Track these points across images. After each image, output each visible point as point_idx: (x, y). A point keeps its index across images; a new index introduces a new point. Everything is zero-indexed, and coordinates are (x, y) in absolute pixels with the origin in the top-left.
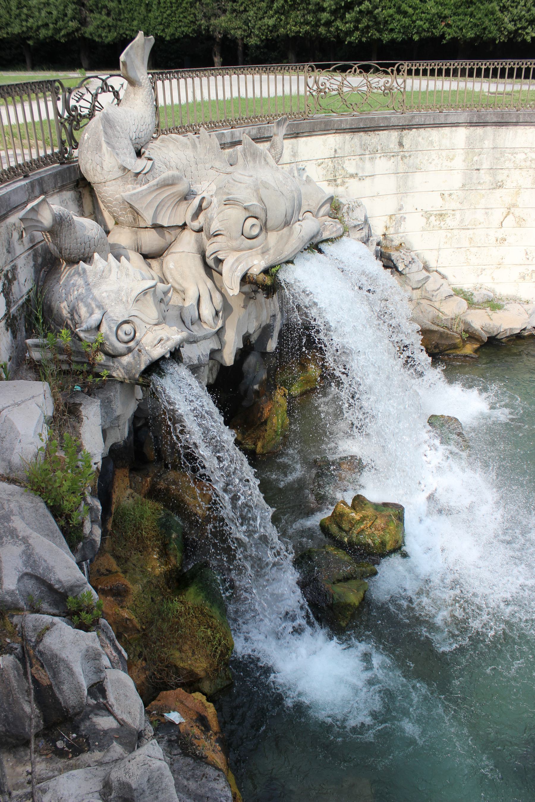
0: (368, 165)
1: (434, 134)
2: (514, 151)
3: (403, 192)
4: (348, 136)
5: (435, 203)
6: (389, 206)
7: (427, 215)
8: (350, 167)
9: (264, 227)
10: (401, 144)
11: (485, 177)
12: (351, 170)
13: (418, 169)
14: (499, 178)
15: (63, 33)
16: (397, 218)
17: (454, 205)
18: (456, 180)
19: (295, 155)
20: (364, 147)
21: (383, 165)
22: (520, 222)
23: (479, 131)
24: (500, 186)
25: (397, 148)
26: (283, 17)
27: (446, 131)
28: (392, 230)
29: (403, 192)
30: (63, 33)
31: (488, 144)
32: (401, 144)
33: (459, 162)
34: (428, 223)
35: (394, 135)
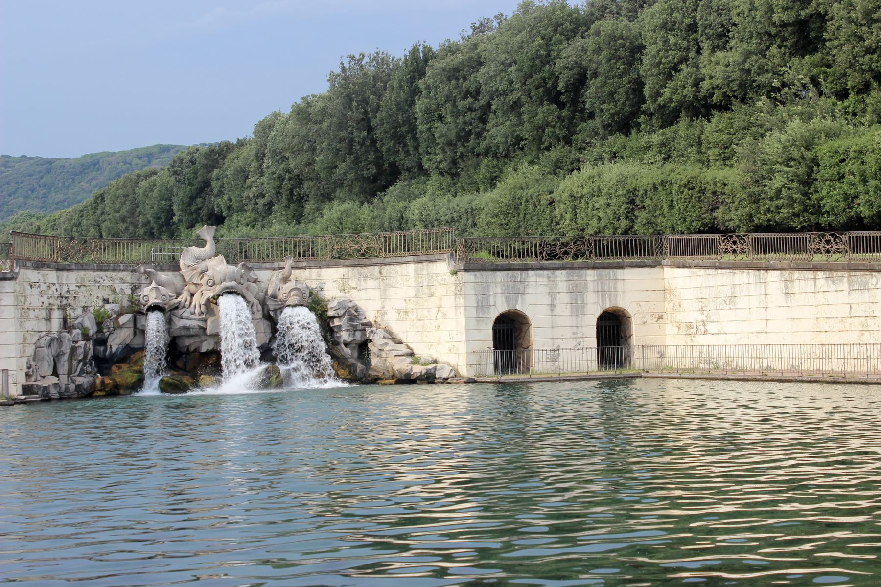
0: (363, 283)
1: (398, 268)
2: (437, 275)
3: (384, 298)
4: (350, 269)
5: (402, 305)
6: (378, 307)
7: (399, 312)
8: (353, 283)
9: (214, 284)
10: (381, 273)
11: (425, 290)
12: (354, 285)
13: (391, 286)
14: (432, 290)
15: (619, 231)
16: (382, 312)
17: (412, 306)
18: (411, 292)
19: (319, 276)
20: (360, 274)
21: (371, 283)
22: (445, 316)
23: (420, 265)
24: (432, 295)
25: (379, 275)
26: (753, 207)
27: (404, 266)
28: (379, 319)
29: (384, 298)
30: (619, 231)
31: (425, 272)
32: (381, 273)
33: (412, 282)
34: (400, 316)
35: (377, 268)
